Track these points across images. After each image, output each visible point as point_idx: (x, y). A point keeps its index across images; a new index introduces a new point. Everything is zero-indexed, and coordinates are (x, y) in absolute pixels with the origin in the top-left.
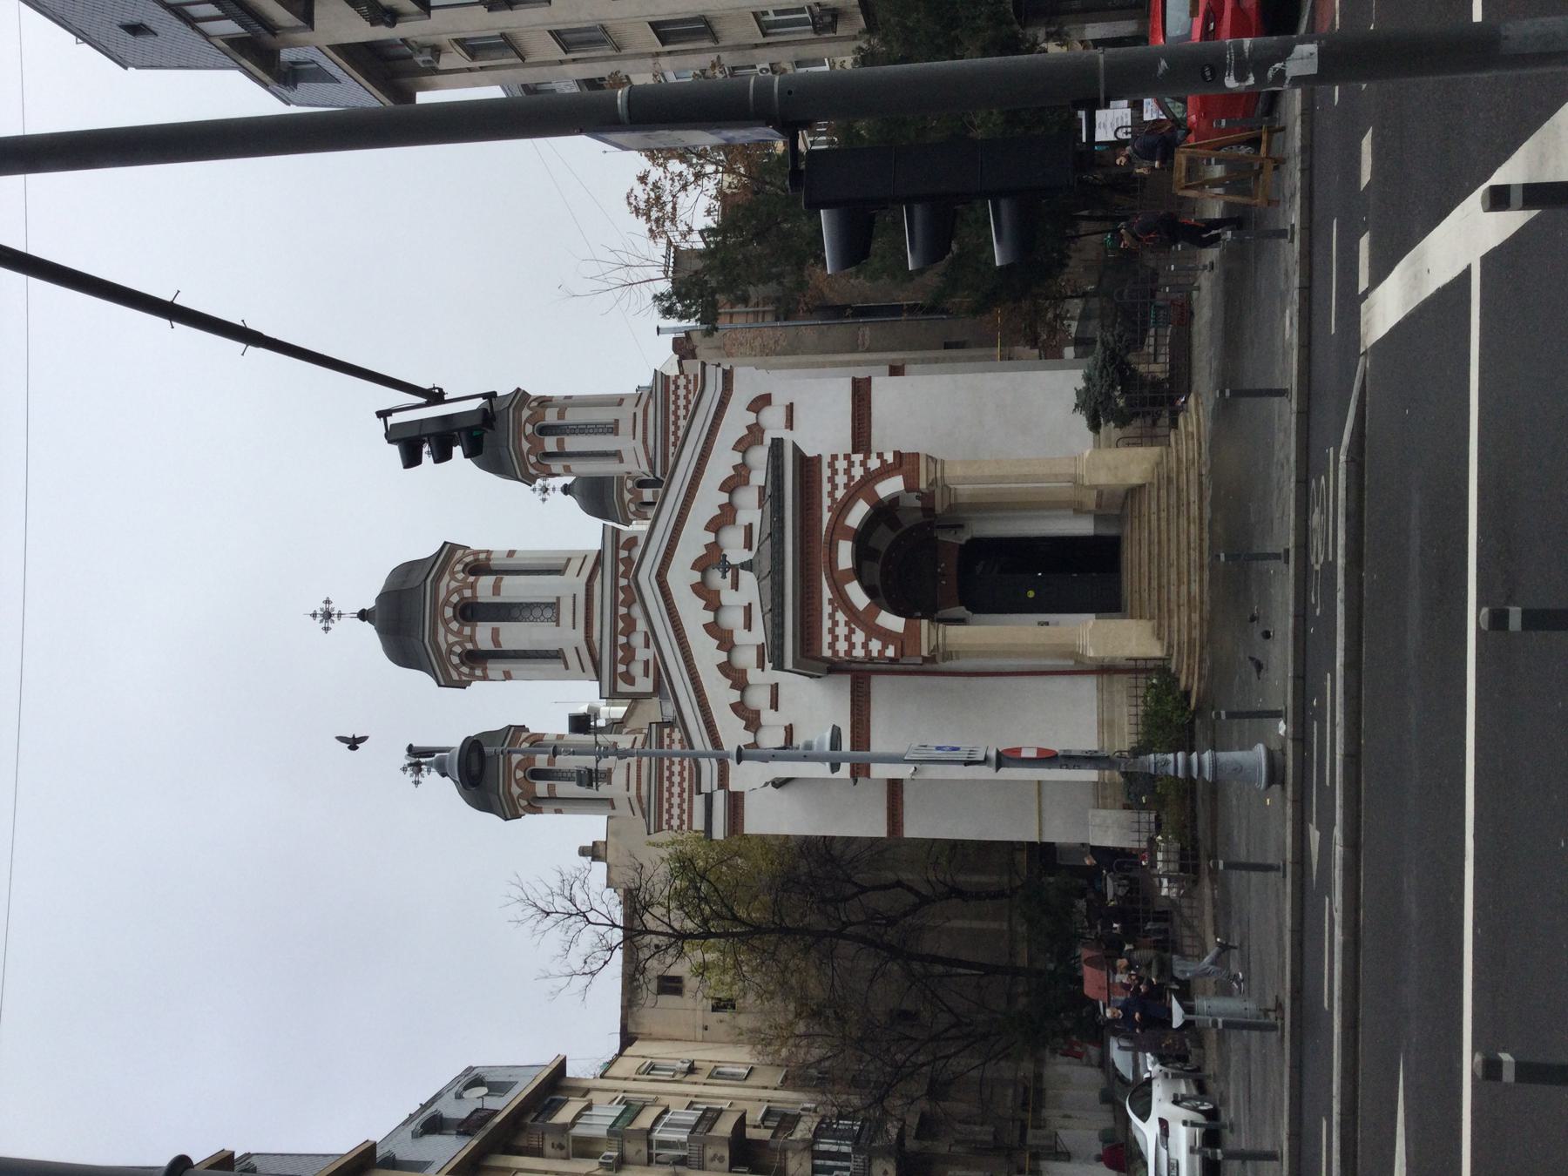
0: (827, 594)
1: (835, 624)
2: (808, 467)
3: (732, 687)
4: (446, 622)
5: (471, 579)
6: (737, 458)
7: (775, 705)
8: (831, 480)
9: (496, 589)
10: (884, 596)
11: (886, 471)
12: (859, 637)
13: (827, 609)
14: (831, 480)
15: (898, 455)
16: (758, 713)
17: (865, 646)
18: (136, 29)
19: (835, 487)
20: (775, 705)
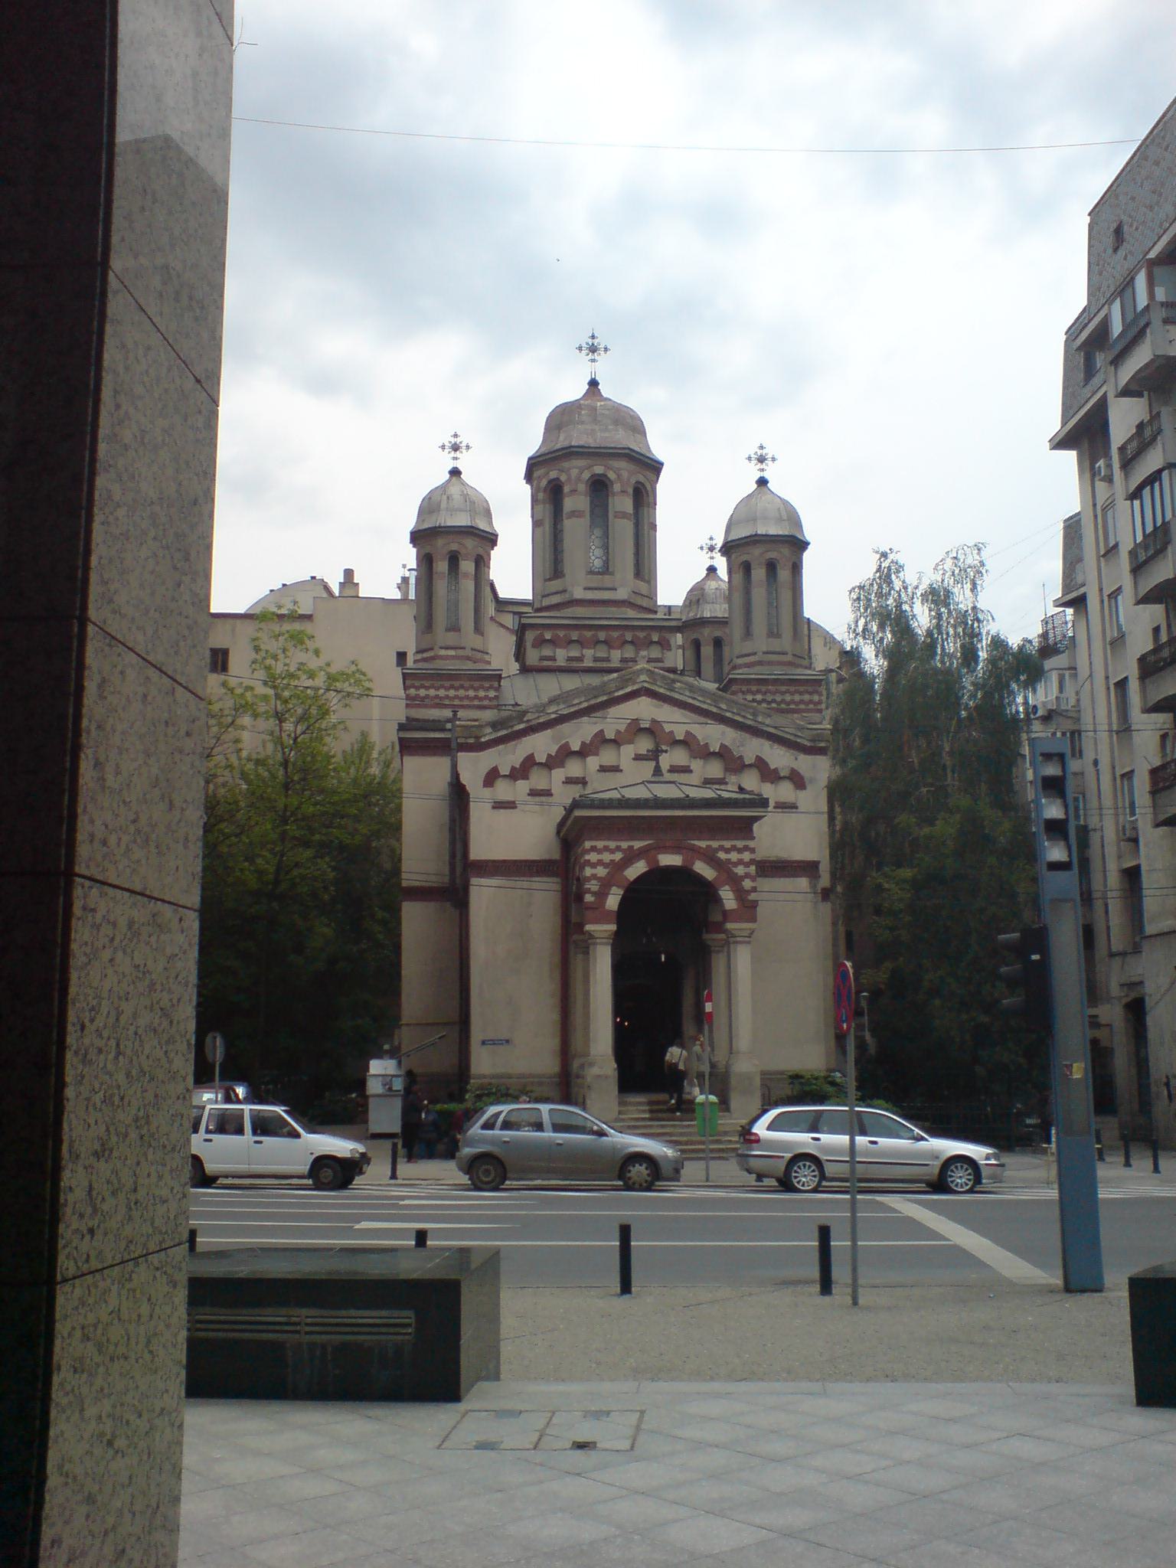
0: (638, 844)
1: (612, 852)
2: (743, 828)
3: (549, 756)
5: (630, 491)
6: (749, 759)
7: (533, 793)
8: (734, 848)
9: (623, 515)
10: (634, 893)
11: (741, 894)
12: (601, 872)
13: (625, 845)
14: (734, 848)
15: (754, 905)
16: (526, 777)
17: (594, 877)
19: (727, 851)
20: (533, 793)
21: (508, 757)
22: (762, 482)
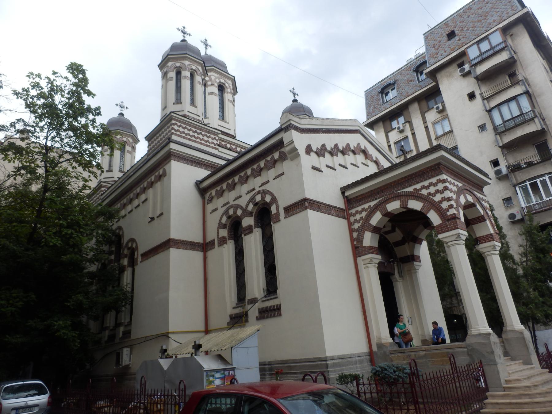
4: (219, 78)
18: (451, 35)
21: (317, 141)
22: (295, 101)
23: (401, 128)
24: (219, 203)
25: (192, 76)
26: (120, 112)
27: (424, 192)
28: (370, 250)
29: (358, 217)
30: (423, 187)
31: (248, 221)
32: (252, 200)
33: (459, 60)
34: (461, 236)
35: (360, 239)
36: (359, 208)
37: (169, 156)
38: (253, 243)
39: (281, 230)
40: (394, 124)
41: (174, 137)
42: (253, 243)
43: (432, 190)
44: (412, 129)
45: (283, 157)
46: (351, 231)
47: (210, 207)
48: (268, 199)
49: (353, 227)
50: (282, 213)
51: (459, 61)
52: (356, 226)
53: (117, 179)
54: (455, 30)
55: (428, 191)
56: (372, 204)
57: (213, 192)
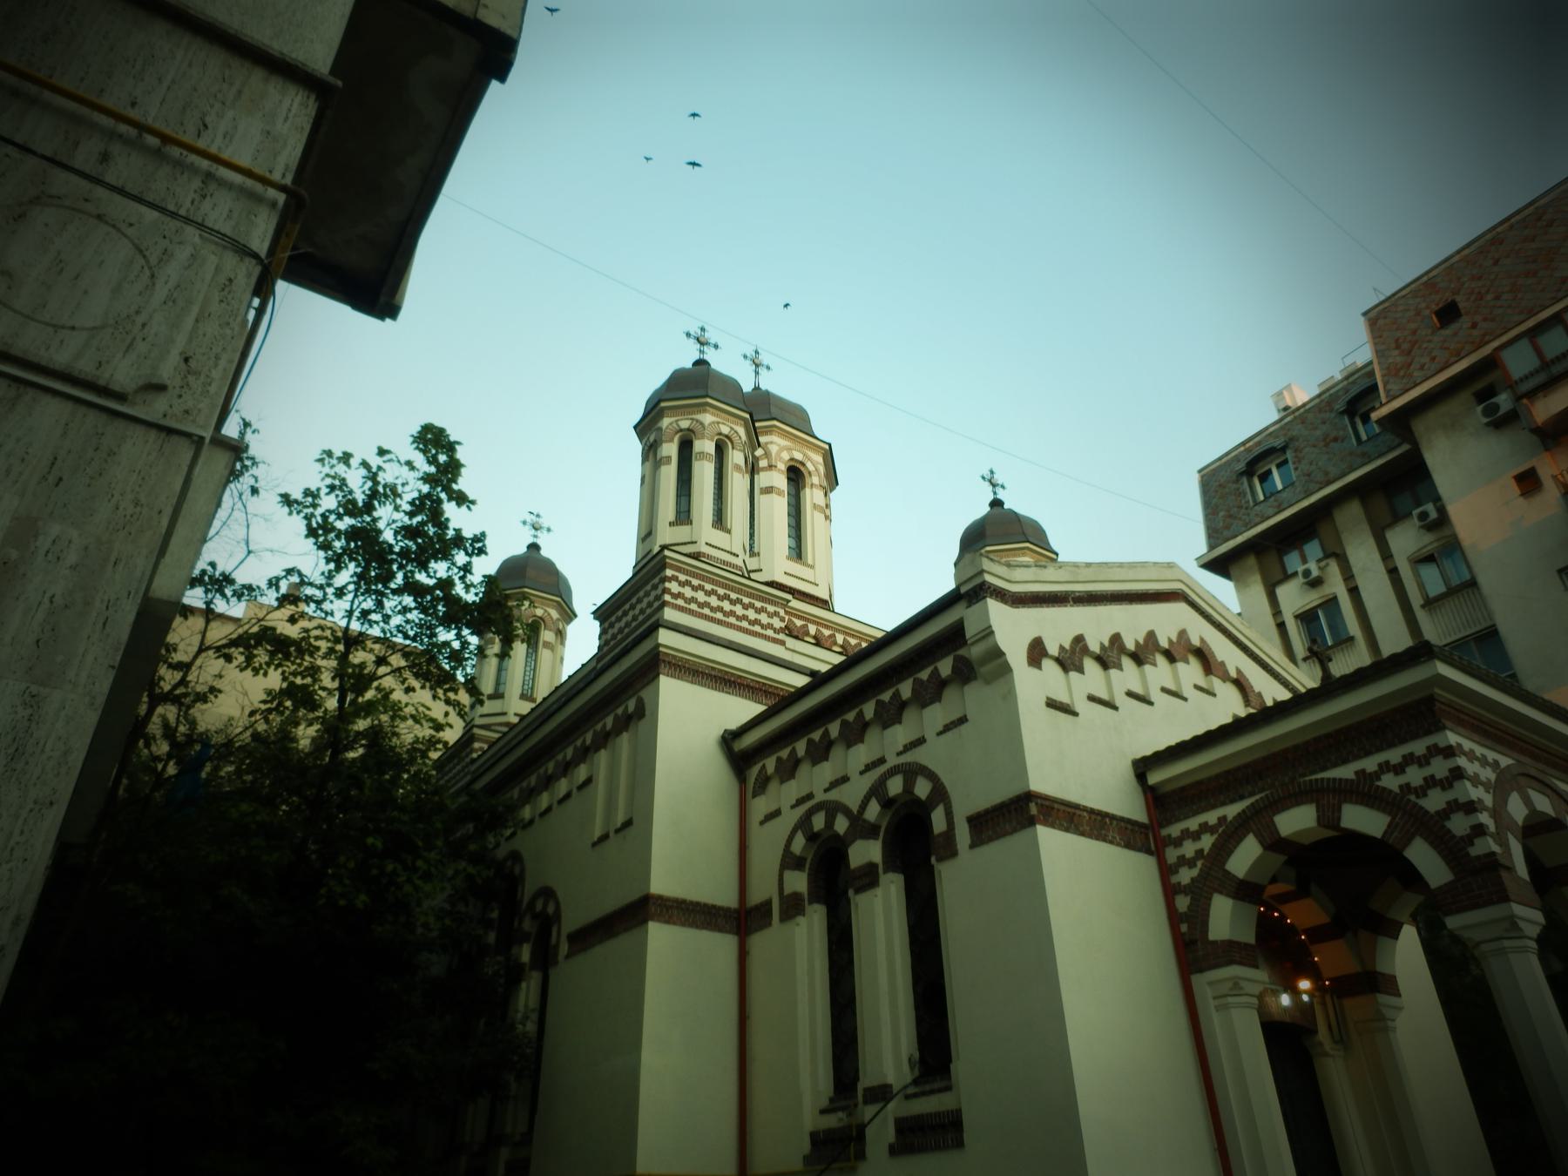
4: (789, 449)
18: (1449, 313)
21: (1058, 626)
22: (996, 503)
23: (1315, 573)
24: (785, 794)
25: (720, 449)
26: (531, 540)
27: (1390, 782)
28: (1230, 952)
29: (1189, 849)
30: (1385, 767)
31: (865, 852)
32: (877, 790)
33: (1481, 383)
34: (1522, 924)
35: (1199, 915)
36: (1193, 824)
37: (654, 665)
38: (881, 914)
39: (962, 879)
40: (1293, 561)
41: (669, 614)
42: (881, 914)
43: (1414, 776)
44: (1348, 576)
45: (965, 673)
46: (1170, 891)
47: (760, 806)
48: (922, 789)
49: (1174, 879)
50: (963, 834)
51: (1479, 385)
52: (1185, 876)
53: (515, 720)
54: (1458, 299)
55: (1402, 779)
56: (1232, 811)
57: (770, 764)
